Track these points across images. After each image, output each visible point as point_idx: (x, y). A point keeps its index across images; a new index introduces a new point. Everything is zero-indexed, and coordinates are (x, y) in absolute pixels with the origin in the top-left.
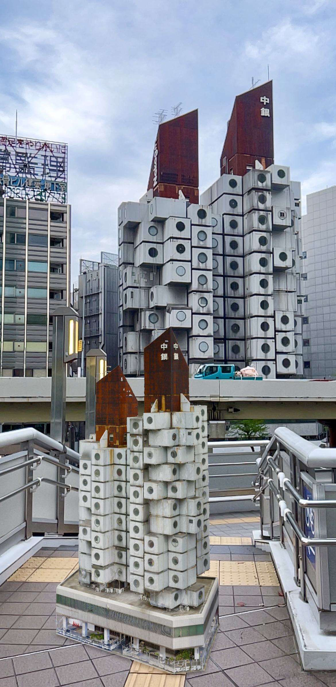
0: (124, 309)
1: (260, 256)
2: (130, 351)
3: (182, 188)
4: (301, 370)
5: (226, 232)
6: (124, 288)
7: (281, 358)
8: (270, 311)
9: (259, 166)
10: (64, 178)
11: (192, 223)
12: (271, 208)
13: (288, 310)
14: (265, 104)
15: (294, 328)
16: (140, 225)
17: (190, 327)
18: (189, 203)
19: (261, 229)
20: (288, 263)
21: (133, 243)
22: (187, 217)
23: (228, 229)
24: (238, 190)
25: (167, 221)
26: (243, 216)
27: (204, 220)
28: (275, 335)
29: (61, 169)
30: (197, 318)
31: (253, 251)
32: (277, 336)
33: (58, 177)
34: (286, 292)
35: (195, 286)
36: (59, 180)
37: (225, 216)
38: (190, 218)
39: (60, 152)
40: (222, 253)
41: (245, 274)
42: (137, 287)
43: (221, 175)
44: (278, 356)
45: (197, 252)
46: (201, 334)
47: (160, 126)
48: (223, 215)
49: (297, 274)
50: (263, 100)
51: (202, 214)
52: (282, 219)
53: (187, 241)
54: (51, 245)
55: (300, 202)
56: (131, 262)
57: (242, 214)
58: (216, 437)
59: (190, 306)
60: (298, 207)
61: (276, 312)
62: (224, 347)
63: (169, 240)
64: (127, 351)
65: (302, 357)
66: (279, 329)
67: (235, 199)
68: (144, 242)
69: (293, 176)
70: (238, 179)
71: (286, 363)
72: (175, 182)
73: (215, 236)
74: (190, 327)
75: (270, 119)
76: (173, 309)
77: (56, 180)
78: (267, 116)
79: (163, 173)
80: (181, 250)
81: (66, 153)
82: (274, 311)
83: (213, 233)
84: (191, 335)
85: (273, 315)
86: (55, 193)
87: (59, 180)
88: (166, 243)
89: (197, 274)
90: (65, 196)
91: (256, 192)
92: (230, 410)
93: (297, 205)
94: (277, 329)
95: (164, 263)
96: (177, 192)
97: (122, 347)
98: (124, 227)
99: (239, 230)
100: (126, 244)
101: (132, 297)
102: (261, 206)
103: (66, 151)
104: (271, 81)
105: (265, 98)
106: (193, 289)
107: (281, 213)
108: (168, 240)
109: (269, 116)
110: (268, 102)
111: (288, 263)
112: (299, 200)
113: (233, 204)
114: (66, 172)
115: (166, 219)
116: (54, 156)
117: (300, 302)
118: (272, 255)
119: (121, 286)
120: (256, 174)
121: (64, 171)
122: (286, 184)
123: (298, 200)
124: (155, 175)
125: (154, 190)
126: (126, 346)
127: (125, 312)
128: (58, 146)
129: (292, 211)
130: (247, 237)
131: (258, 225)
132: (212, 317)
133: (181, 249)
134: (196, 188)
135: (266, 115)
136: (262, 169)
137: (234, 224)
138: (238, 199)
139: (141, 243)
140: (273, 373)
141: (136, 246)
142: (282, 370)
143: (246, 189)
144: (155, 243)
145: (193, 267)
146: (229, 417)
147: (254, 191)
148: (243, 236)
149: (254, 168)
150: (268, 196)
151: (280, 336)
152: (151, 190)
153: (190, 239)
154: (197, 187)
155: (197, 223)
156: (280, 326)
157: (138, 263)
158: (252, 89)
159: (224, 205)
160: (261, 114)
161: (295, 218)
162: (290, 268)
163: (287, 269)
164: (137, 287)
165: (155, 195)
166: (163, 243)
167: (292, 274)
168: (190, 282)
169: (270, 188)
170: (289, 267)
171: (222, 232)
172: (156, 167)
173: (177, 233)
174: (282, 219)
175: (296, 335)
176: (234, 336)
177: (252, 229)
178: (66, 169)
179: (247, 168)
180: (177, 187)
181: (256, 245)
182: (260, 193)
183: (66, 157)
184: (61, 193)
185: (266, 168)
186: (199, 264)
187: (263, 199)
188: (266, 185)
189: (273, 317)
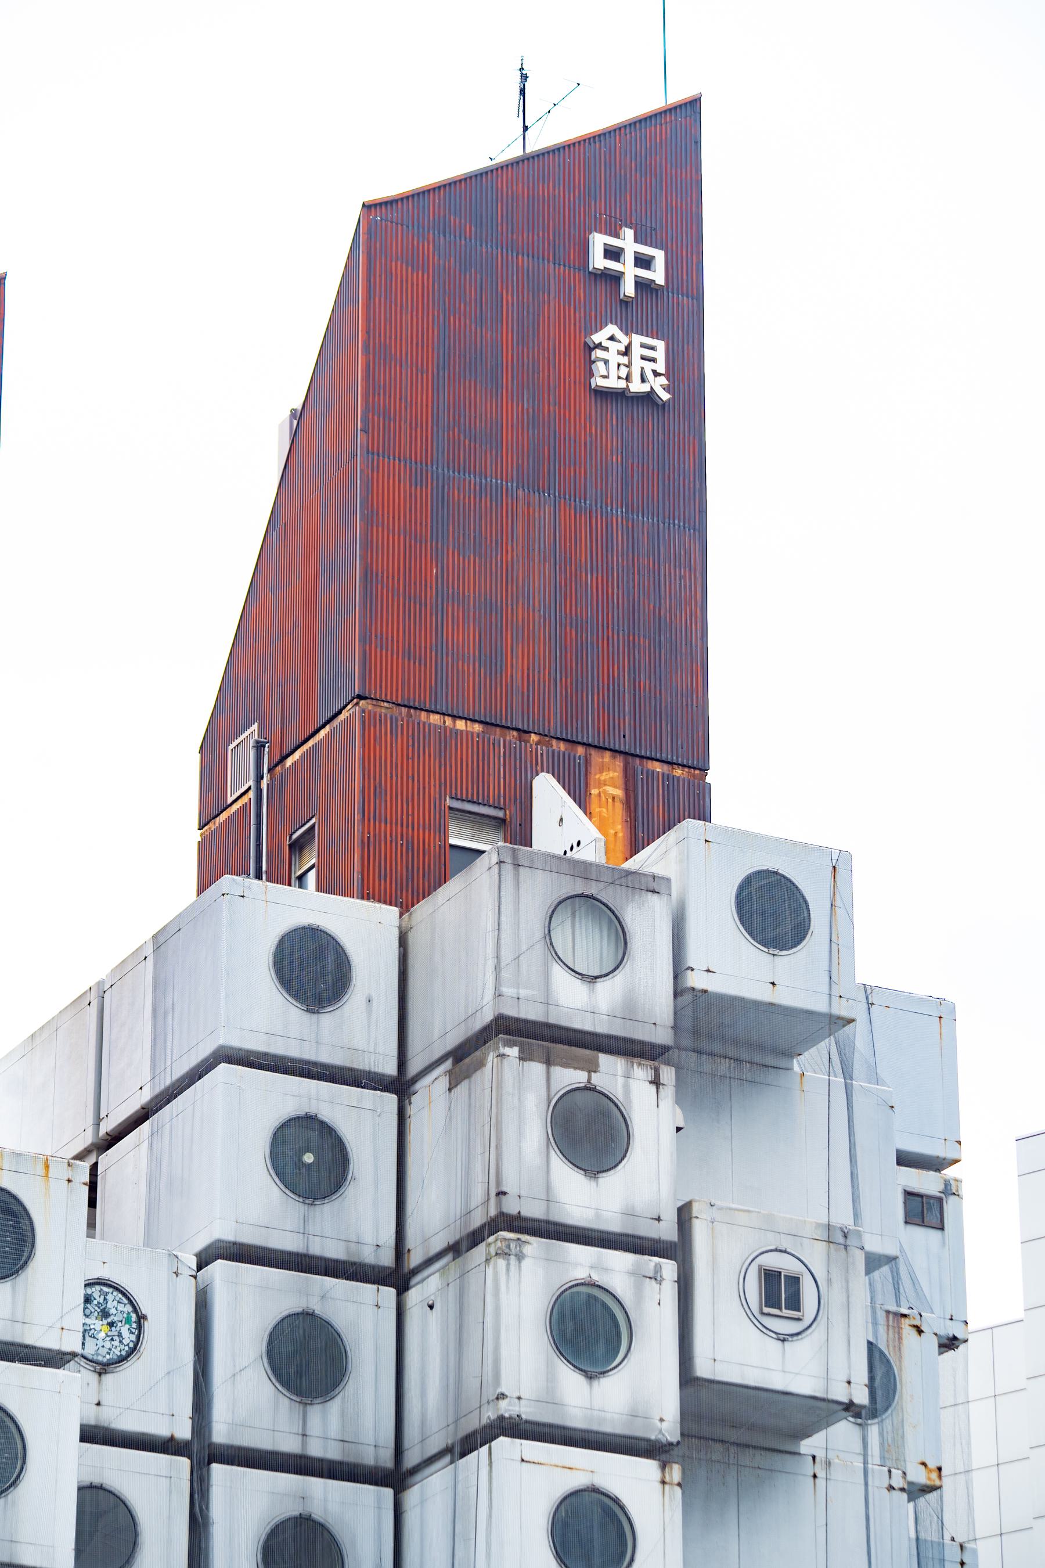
5: (221, 1433)
12: (670, 1218)
14: (629, 288)
19: (576, 1419)
24: (359, 1041)
37: (219, 1267)
43: (202, 887)
48: (204, 1260)
50: (613, 254)
52: (783, 1339)
55: (950, 1190)
57: (387, 1259)
60: (934, 1234)
67: (327, 1114)
78: (649, 397)
83: (91, 1435)
104: (693, 105)
105: (628, 242)
107: (770, 1278)
109: (665, 396)
110: (658, 275)
112: (950, 1172)
123: (934, 1164)
129: (874, 1262)
131: (551, 1378)
135: (637, 387)
136: (592, 853)
147: (514, 1052)
158: (516, 152)
160: (591, 374)
169: (662, 1036)
171: (184, 1431)
174: (783, 1339)
177: (489, 1414)
179: (452, 841)
182: (569, 1077)
185: (634, 848)
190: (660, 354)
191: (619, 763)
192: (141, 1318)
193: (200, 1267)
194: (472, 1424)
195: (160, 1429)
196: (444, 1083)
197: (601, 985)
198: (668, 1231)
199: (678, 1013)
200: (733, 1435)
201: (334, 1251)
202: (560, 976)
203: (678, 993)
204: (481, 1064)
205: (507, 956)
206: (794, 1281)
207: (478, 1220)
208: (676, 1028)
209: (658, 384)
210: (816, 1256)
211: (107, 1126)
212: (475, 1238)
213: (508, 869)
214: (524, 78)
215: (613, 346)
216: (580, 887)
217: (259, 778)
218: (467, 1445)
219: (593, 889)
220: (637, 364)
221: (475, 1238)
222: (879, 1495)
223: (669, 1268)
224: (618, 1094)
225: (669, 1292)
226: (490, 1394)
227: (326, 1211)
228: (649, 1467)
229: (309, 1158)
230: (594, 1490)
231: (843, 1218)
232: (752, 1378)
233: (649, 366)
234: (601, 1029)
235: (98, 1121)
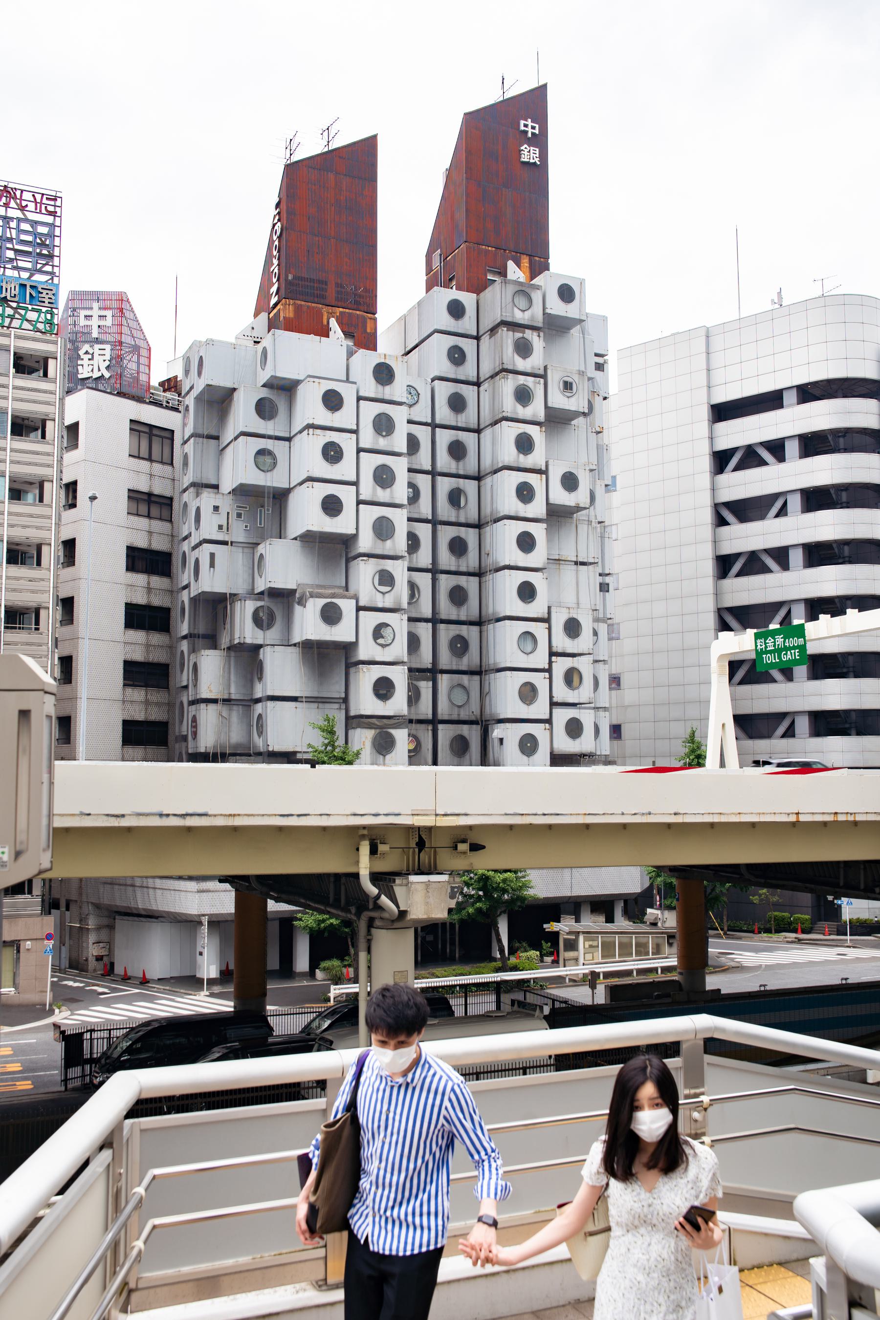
0: (192, 596)
1: (514, 479)
2: (205, 695)
3: (338, 314)
4: (605, 746)
5: (438, 421)
6: (193, 544)
7: (562, 716)
8: (537, 608)
9: (515, 272)
10: (52, 274)
11: (361, 394)
12: (542, 369)
14: (530, 135)
15: (591, 647)
16: (236, 394)
17: (354, 640)
18: (354, 348)
19: (521, 417)
20: (580, 497)
21: (217, 438)
22: (347, 380)
23: (444, 414)
25: (301, 388)
26: (478, 384)
27: (387, 388)
28: (550, 663)
29: (45, 252)
30: (370, 620)
31: (500, 465)
32: (553, 664)
33: (34, 271)
34: (576, 563)
35: (366, 542)
36: (39, 278)
38: (355, 383)
39: (44, 211)
40: (430, 468)
41: (482, 522)
42: (225, 543)
44: (557, 711)
45: (370, 462)
46: (378, 659)
47: (287, 167)
48: (433, 380)
49: (600, 523)
50: (526, 126)
52: (568, 397)
53: (348, 435)
54: (13, 433)
55: (605, 362)
56: (214, 482)
57: (475, 380)
58: (425, 917)
59: (352, 590)
60: (601, 373)
61: (553, 610)
62: (431, 690)
63: (306, 432)
64: (198, 697)
65: (607, 713)
66: (560, 650)
67: (460, 345)
70: (468, 299)
71: (574, 728)
72: (321, 298)
74: (354, 640)
75: (540, 170)
76: (312, 596)
77: (33, 278)
79: (294, 278)
80: (332, 456)
81: (58, 214)
82: (549, 608)
83: (410, 422)
84: (354, 660)
85: (546, 616)
86: (26, 309)
87: (39, 278)
88: (296, 440)
89: (370, 514)
90: (52, 317)
92: (462, 847)
93: (599, 367)
94: (554, 650)
95: (291, 486)
96: (325, 322)
97: (186, 687)
99: (469, 417)
101: (212, 565)
102: (521, 364)
103: (58, 210)
104: (545, 86)
105: (529, 122)
108: (300, 432)
109: (539, 163)
110: (537, 131)
111: (580, 497)
112: (605, 358)
113: (456, 356)
114: (56, 261)
115: (297, 383)
116: (26, 220)
117: (604, 588)
118: (544, 476)
119: (186, 538)
121: (51, 256)
122: (577, 317)
125: (272, 315)
126: (195, 686)
127: (194, 601)
128: (38, 197)
129: (590, 379)
130: (487, 434)
131: (515, 407)
132: (405, 617)
133: (332, 453)
134: (372, 315)
135: (532, 161)
137: (457, 403)
138: (469, 346)
139: (236, 438)
140: (543, 752)
142: (566, 745)
143: (486, 324)
144: (270, 437)
145: (362, 497)
146: (460, 864)
147: (505, 329)
148: (478, 431)
149: (506, 276)
150: (537, 342)
151: (561, 666)
152: (264, 316)
153: (355, 432)
154: (374, 314)
155: (372, 395)
156: (562, 642)
157: (227, 485)
158: (501, 99)
161: (596, 396)
162: (585, 508)
163: (578, 512)
164: (225, 543)
165: (272, 325)
166: (289, 439)
167: (590, 522)
168: (354, 532)
169: (540, 325)
170: (582, 505)
172: (275, 262)
173: (323, 416)
175: (597, 665)
176: (454, 663)
177: (501, 416)
178: (56, 253)
180: (325, 310)
181: (509, 453)
182: (519, 335)
183: (57, 223)
184: (44, 309)
185: (532, 279)
186: (374, 490)
187: (523, 349)
188: (532, 318)
189: (547, 620)
190: (537, 152)
191: (528, 258)
192: (419, 394)
193: (432, 381)
194: (497, 418)
195: (424, 420)
196: (488, 337)
197: (526, 313)
198: (541, 372)
199: (544, 319)
200: (558, 420)
201: (463, 378)
202: (516, 309)
203: (544, 314)
204: (498, 332)
205: (503, 305)
206: (571, 384)
207: (497, 370)
208: (543, 323)
209: (537, 160)
210: (576, 378)
211: (408, 349)
212: (497, 374)
213: (503, 284)
214: (503, 79)
215: (526, 150)
216: (521, 288)
217: (441, 263)
218: (496, 423)
219: (523, 289)
220: (532, 155)
221: (497, 374)
222: (590, 434)
223: (542, 381)
224: (530, 339)
225: (542, 386)
226: (501, 411)
227: (461, 368)
228: (537, 428)
229: (456, 356)
230: (525, 433)
231: (582, 369)
232: (561, 407)
233: (535, 155)
234: (526, 323)
235: (405, 348)
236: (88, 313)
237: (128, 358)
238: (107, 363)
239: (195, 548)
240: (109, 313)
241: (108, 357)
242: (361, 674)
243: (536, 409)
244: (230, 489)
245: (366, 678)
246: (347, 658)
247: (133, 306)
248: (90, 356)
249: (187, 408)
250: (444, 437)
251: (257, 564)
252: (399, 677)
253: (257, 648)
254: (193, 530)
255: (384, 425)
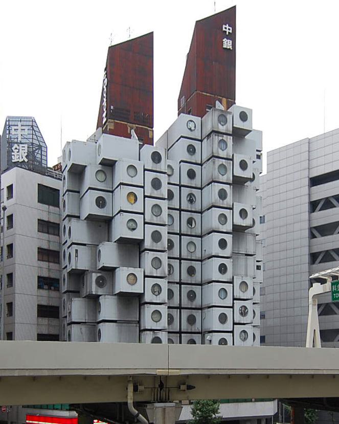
5: (182, 184)
13: (246, 275)
14: (227, 33)
17: (143, 292)
21: (78, 192)
23: (185, 180)
30: (150, 282)
48: (180, 162)
50: (226, 28)
51: (156, 157)
68: (90, 188)
69: (256, 123)
70: (197, 120)
73: (172, 188)
74: (143, 292)
75: (232, 53)
78: (230, 49)
83: (169, 183)
84: (143, 302)
89: (150, 229)
91: (215, 135)
98: (68, 171)
100: (70, 193)
101: (77, 256)
105: (227, 26)
106: (146, 247)
109: (231, 49)
110: (231, 31)
113: (191, 150)
120: (217, 114)
124: (105, 110)
135: (228, 47)
137: (191, 174)
138: (197, 145)
141: (83, 194)
143: (205, 134)
159: (180, 151)
160: (223, 45)
181: (215, 198)
185: (228, 108)
198: (231, 157)
201: (194, 161)
209: (231, 47)
223: (231, 162)
228: (229, 186)
236: (16, 128)
237: (36, 152)
238: (26, 154)
239: (69, 247)
240: (26, 128)
241: (26, 151)
242: (146, 309)
243: (228, 177)
244: (84, 218)
245: (148, 310)
246: (140, 301)
247: (38, 125)
248: (17, 150)
249: (64, 178)
250: (185, 192)
251: (96, 255)
252: (163, 310)
253: (97, 297)
254: (68, 239)
255: (156, 184)
